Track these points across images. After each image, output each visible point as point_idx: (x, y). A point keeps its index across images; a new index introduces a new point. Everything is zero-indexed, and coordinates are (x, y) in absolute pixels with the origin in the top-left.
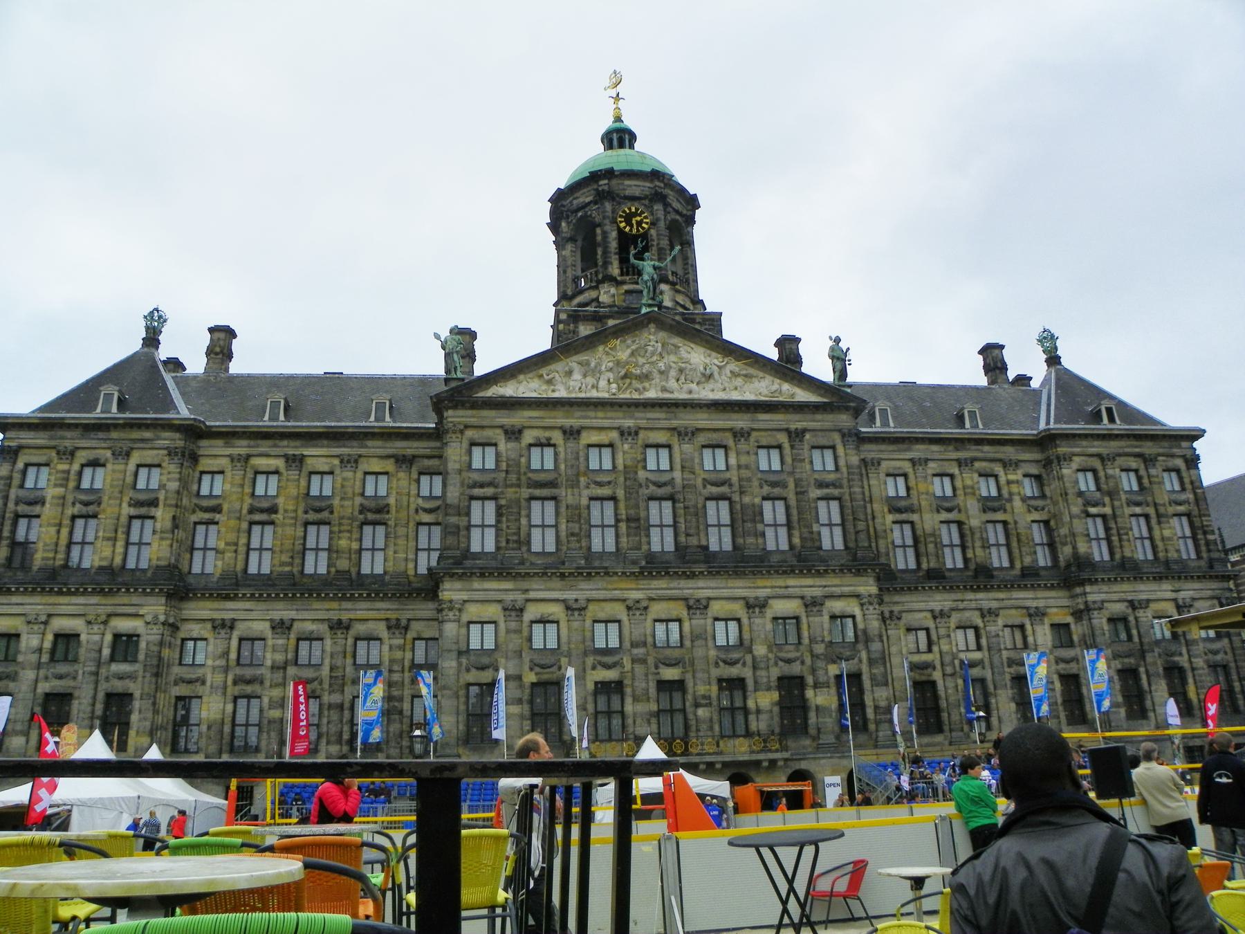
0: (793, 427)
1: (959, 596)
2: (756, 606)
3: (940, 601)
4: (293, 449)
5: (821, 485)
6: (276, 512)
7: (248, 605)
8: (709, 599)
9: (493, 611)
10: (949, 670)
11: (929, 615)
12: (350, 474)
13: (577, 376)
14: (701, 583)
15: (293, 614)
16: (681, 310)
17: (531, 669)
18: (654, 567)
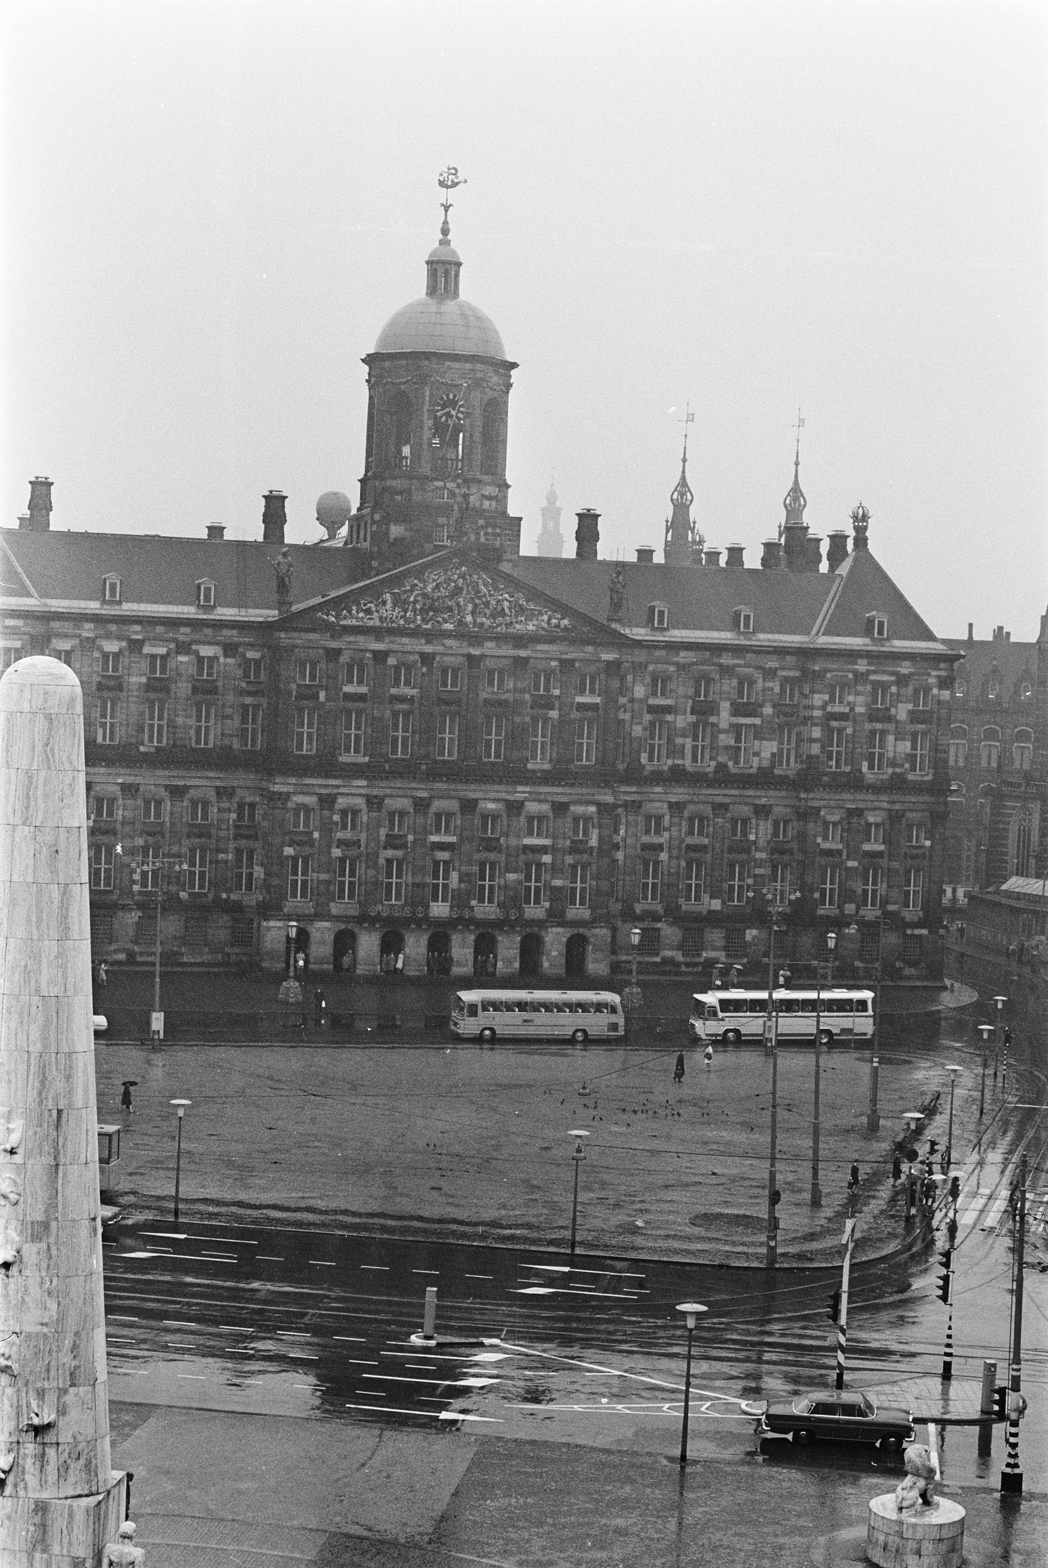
0: (565, 656)
1: (696, 791)
2: (514, 808)
3: (678, 794)
4: (136, 632)
5: (583, 707)
6: (121, 690)
7: (102, 770)
8: (476, 800)
9: (310, 800)
10: (675, 853)
11: (665, 806)
12: (182, 658)
13: (389, 605)
14: (473, 787)
15: (139, 780)
16: (486, 504)
17: (338, 847)
18: (438, 772)
